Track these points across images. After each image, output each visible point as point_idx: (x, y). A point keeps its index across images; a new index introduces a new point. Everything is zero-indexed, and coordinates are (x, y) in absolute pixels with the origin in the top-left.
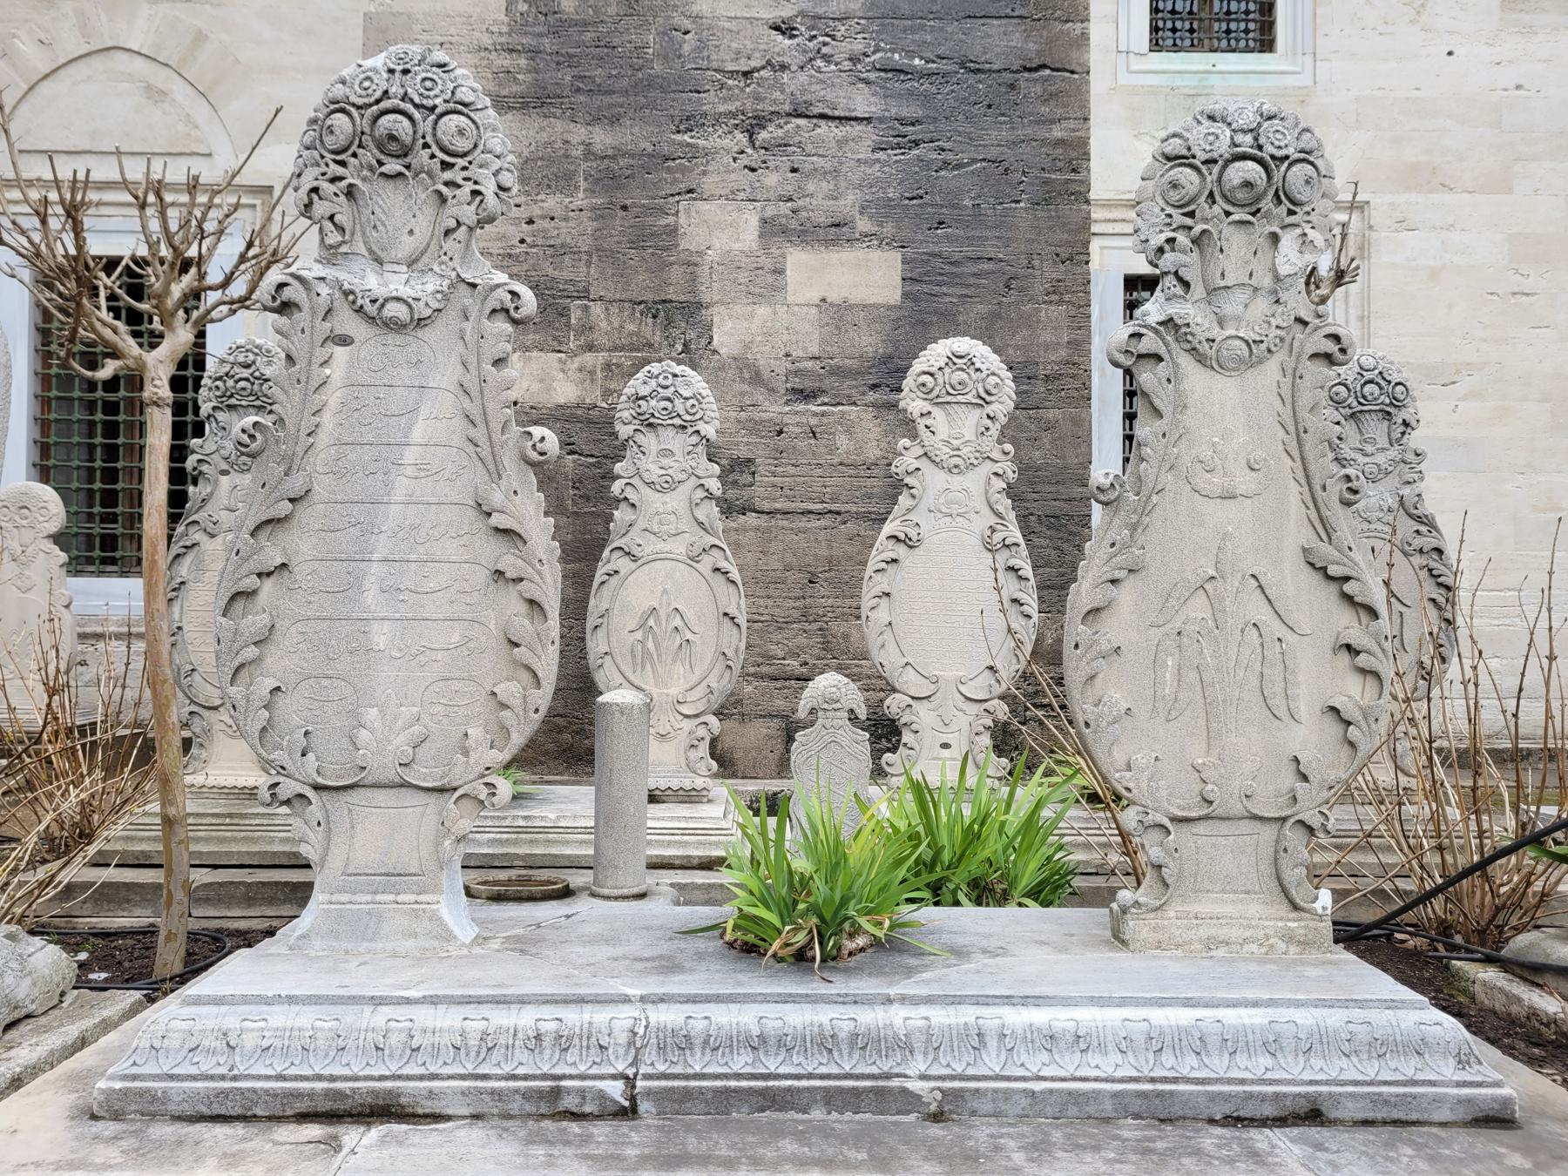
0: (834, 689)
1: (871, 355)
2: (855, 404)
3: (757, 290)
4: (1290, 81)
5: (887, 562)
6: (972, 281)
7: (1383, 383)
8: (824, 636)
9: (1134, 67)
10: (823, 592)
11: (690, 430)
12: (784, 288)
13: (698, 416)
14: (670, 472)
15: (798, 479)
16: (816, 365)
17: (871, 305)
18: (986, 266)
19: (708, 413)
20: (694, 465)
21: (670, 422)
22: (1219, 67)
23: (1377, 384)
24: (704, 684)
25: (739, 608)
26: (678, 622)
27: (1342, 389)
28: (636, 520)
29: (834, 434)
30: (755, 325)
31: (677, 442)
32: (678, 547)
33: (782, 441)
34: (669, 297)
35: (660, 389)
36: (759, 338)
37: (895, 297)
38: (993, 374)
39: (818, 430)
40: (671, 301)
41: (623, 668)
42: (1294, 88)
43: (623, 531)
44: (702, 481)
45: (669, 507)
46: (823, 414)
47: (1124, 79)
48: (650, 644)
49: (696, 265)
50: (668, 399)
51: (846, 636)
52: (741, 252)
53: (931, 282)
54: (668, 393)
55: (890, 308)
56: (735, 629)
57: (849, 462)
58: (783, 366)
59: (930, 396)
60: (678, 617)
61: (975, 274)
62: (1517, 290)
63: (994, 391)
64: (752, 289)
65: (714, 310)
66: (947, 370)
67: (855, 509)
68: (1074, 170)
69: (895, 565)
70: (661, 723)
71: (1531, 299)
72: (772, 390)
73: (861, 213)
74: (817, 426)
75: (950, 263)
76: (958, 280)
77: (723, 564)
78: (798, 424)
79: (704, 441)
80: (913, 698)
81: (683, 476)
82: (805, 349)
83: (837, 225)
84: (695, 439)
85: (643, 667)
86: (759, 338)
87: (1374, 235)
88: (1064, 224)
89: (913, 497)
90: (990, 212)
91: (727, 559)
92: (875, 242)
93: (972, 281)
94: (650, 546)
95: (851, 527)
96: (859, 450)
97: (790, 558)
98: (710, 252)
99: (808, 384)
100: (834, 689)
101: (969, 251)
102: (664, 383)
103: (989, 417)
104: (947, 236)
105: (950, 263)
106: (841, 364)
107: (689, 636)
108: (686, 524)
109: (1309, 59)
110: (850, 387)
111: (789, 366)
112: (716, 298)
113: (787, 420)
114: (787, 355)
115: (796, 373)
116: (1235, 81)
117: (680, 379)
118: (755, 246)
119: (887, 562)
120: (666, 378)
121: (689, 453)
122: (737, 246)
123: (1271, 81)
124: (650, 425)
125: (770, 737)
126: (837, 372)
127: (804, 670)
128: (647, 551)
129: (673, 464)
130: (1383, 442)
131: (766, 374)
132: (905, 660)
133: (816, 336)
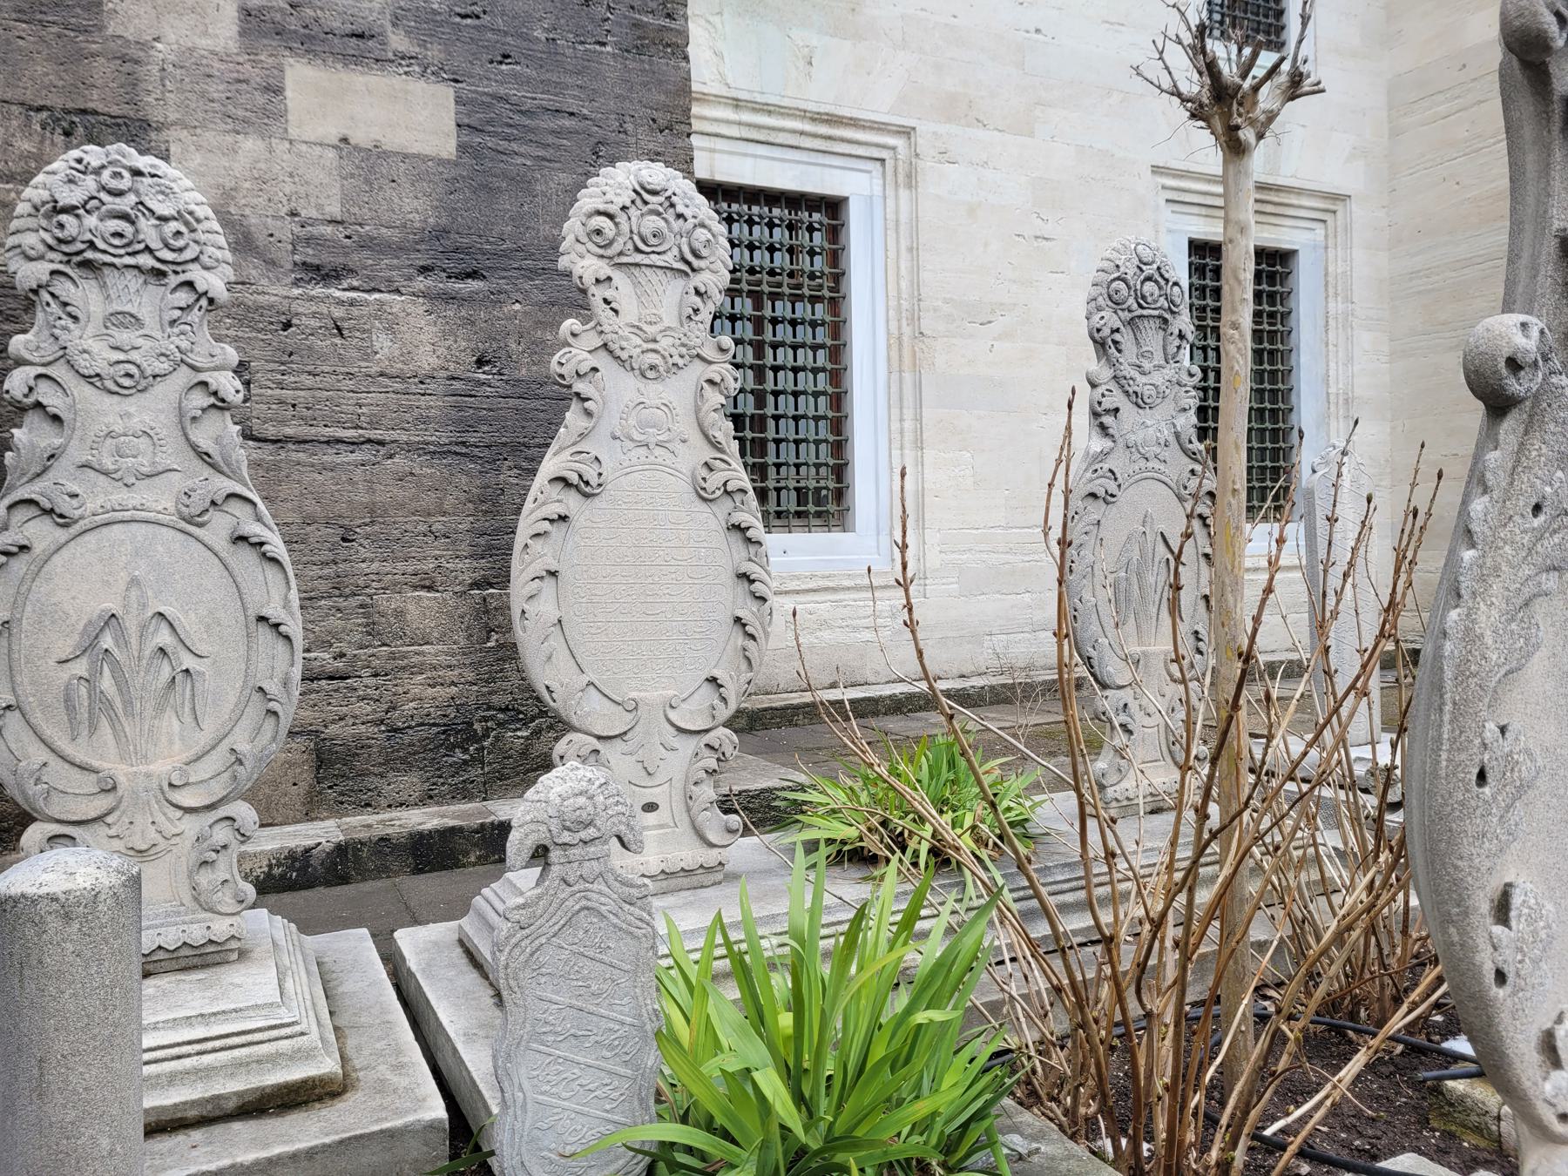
0: (582, 800)
1: (417, 225)
2: (397, 291)
3: (240, 113)
5: (552, 521)
6: (551, 139)
7: (1162, 282)
8: (367, 615)
10: (364, 554)
11: (173, 280)
12: (282, 115)
13: (188, 255)
14: (135, 356)
15: (318, 394)
16: (340, 233)
17: (415, 156)
18: (568, 123)
19: (210, 250)
20: (185, 345)
21: (129, 260)
23: (1156, 282)
24: (224, 746)
25: (286, 604)
26: (164, 637)
27: (1122, 285)
28: (63, 449)
29: (369, 331)
30: (240, 164)
31: (147, 301)
32: (160, 499)
33: (291, 338)
34: (91, 105)
35: (104, 196)
36: (247, 185)
37: (446, 146)
38: (703, 225)
39: (346, 325)
40: (95, 113)
41: (48, 731)
43: (38, 469)
44: (203, 377)
45: (136, 423)
46: (352, 303)
48: (107, 683)
49: (137, 62)
50: (124, 217)
51: (400, 614)
52: (212, 52)
53: (495, 135)
54: (126, 204)
55: (441, 162)
56: (281, 646)
57: (394, 372)
58: (287, 230)
59: (609, 252)
60: (165, 631)
61: (553, 132)
62: (1039, 234)
63: (704, 252)
64: (231, 109)
65: (172, 134)
66: (633, 212)
67: (405, 438)
68: (669, 16)
69: (563, 525)
70: (137, 828)
71: (1053, 243)
72: (272, 263)
73: (394, 25)
74: (343, 319)
75: (521, 112)
76: (532, 136)
77: (253, 529)
78: (314, 315)
79: (204, 302)
80: (599, 738)
81: (162, 366)
82: (319, 207)
83: (360, 36)
84: (184, 297)
85: (93, 728)
86: (247, 185)
88: (660, 82)
89: (588, 413)
90: (569, 52)
91: (259, 519)
92: (417, 68)
93: (551, 139)
94: (96, 497)
95: (400, 462)
96: (407, 356)
97: (311, 507)
98: (159, 46)
99: (326, 259)
100: (582, 800)
101: (544, 99)
102: (115, 184)
103: (698, 292)
104: (515, 75)
105: (521, 112)
106: (375, 233)
107: (188, 662)
108: (172, 454)
110: (391, 268)
111: (297, 229)
112: (172, 117)
113: (297, 307)
114: (293, 214)
115: (309, 240)
117: (148, 180)
118: (233, 46)
119: (552, 521)
120: (117, 175)
121: (173, 323)
122: (204, 43)
124: (87, 264)
125: (291, 764)
126: (367, 244)
127: (340, 664)
128: (91, 506)
129: (140, 342)
130: (1159, 359)
131: (261, 239)
132: (585, 679)
133: (336, 190)
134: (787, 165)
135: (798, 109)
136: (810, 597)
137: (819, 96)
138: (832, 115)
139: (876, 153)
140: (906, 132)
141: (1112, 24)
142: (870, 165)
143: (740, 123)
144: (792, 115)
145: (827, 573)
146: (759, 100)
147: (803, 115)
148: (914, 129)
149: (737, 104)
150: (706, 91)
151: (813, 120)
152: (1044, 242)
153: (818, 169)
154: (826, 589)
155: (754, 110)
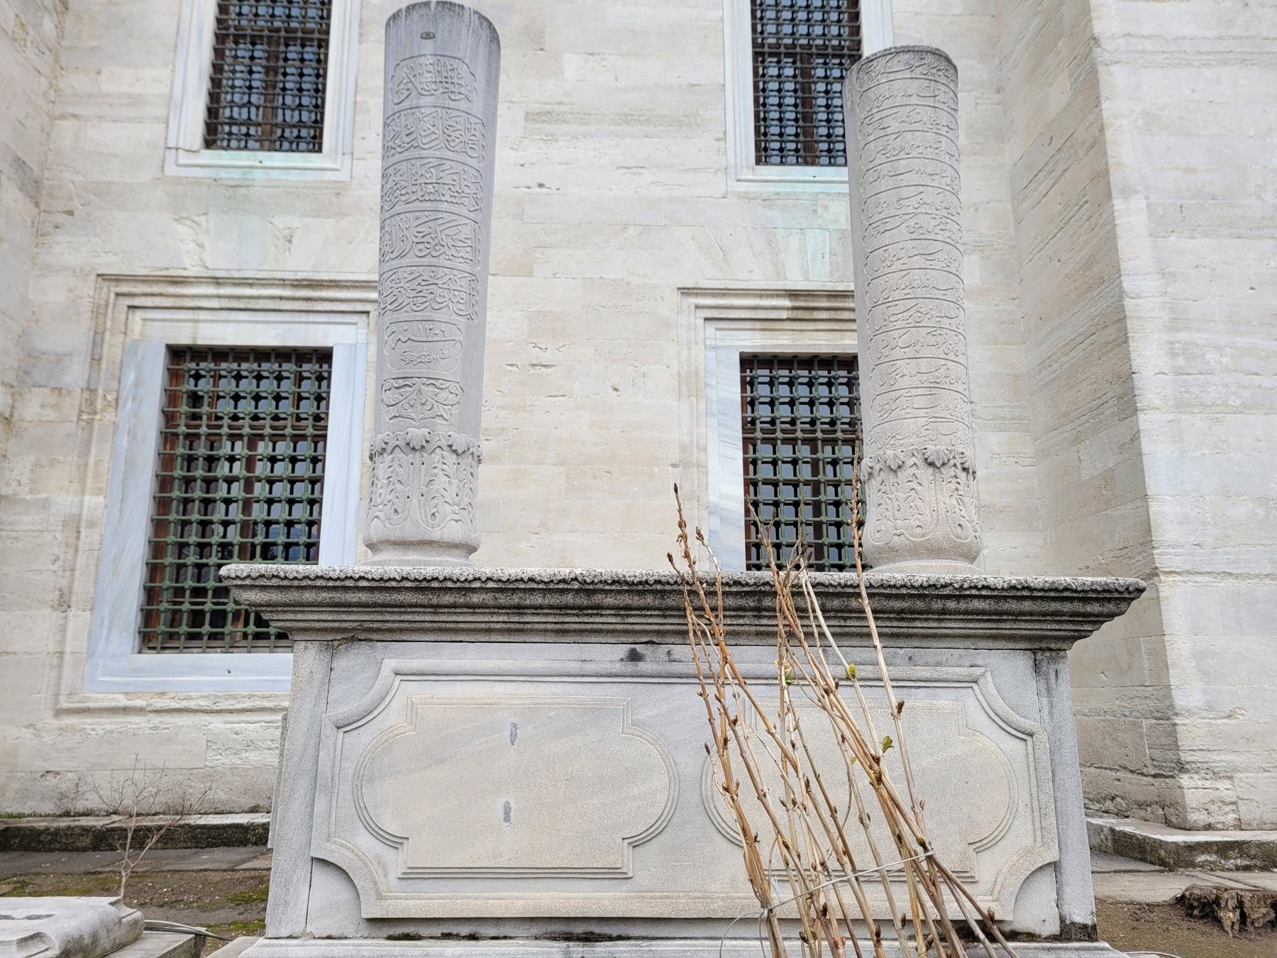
4: (328, 176)
9: (182, 161)
22: (265, 164)
42: (330, 182)
47: (171, 170)
71: (549, 370)
109: (348, 157)
116: (276, 175)
123: (310, 176)
134: (270, 326)
135: (274, 279)
136: (244, 717)
137: (299, 264)
139: (359, 307)
141: (629, 168)
142: (355, 318)
143: (219, 297)
145: (268, 693)
146: (235, 276)
147: (283, 283)
149: (217, 281)
150: (185, 275)
151: (296, 286)
152: (543, 369)
153: (302, 326)
154: (263, 710)
155: (235, 284)
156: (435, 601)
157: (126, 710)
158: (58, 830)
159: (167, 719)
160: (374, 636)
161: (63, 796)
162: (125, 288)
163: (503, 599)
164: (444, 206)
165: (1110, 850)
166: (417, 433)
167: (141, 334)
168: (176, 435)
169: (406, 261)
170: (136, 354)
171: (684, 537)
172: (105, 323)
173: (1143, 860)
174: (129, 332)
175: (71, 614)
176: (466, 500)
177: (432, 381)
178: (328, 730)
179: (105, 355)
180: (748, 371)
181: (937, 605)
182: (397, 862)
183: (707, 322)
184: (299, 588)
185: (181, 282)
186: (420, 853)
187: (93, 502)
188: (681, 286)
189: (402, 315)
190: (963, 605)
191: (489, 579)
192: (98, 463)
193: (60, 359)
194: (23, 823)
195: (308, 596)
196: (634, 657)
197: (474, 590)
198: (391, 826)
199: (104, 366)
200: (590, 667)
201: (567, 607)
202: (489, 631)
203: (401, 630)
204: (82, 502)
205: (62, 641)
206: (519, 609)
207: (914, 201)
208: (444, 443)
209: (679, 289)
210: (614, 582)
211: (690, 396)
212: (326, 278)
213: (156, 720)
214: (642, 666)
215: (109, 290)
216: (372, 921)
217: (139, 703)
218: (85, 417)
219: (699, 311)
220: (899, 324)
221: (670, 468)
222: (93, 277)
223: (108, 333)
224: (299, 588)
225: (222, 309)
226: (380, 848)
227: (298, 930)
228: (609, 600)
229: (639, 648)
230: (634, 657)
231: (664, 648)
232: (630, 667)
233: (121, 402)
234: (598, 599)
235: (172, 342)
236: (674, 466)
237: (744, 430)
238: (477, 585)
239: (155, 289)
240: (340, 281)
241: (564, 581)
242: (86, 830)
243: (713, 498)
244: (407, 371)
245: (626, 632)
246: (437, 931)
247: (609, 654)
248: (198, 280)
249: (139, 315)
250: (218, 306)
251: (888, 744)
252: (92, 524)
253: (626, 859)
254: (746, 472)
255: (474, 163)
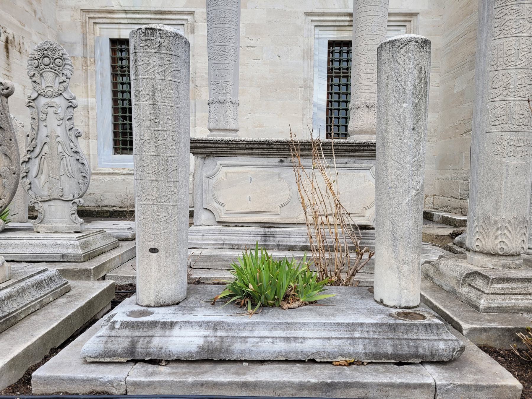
71: (254, 49)
87: (196, 24)
135: (147, 11)
138: (161, 11)
139: (180, 22)
140: (192, 13)
143: (127, 18)
144: (147, 13)
146: (132, 9)
147: (150, 12)
148: (194, 12)
149: (126, 12)
150: (113, 9)
151: (155, 13)
152: (251, 48)
155: (132, 13)
156: (230, 146)
157: (113, 174)
158: (98, 211)
159: (127, 177)
160: (214, 155)
161: (97, 201)
162: (92, 15)
163: (247, 146)
164: (227, 25)
165: (441, 222)
166: (222, 98)
167: (100, 34)
168: (117, 75)
169: (216, 44)
170: (99, 42)
171: (291, 136)
172: (86, 30)
173: (450, 225)
174: (95, 34)
175: (90, 141)
176: (236, 117)
177: (225, 82)
178: (205, 178)
179: (88, 43)
180: (331, 48)
181: (362, 148)
182: (223, 209)
183: (316, 27)
184: (196, 143)
185: (112, 12)
186: (228, 208)
187: (92, 101)
188: (306, 12)
189: (215, 61)
190: (369, 148)
191: (244, 141)
192: (91, 86)
193: (72, 44)
194: (86, 209)
195: (198, 145)
196: (282, 161)
197: (240, 144)
198: (222, 201)
199: (88, 48)
200: (270, 164)
201: (264, 148)
202: (244, 154)
203: (221, 154)
204: (88, 101)
205: (89, 150)
206: (252, 149)
207: (371, 21)
208: (229, 101)
209: (305, 13)
210: (276, 142)
211: (308, 59)
212: (167, 10)
213: (124, 177)
214: (283, 164)
215: (86, 16)
216: (218, 222)
217: (117, 171)
218: (84, 68)
219: (312, 22)
220: (363, 62)
221: (299, 88)
222: (80, 11)
223: (88, 34)
224: (196, 143)
225: (128, 23)
226: (219, 206)
227: (201, 224)
228: (275, 147)
229: (283, 159)
230: (282, 161)
231: (289, 159)
232: (280, 164)
233: (96, 62)
234: (272, 146)
235: (111, 37)
236: (301, 87)
237: (328, 73)
238: (241, 142)
239: (103, 15)
240: (172, 11)
241: (263, 141)
242: (107, 211)
243: (315, 100)
244: (218, 79)
245: (279, 155)
246: (234, 225)
247: (275, 160)
248: (118, 12)
249: (98, 26)
250: (127, 22)
251: (334, 181)
252: (92, 109)
253: (279, 210)
254: (328, 89)
255: (235, 9)
